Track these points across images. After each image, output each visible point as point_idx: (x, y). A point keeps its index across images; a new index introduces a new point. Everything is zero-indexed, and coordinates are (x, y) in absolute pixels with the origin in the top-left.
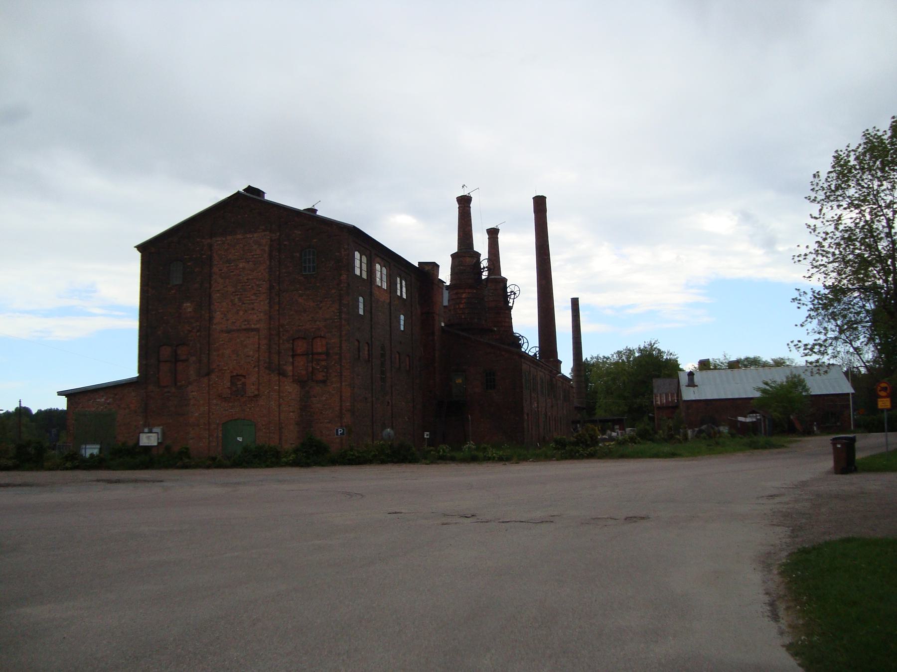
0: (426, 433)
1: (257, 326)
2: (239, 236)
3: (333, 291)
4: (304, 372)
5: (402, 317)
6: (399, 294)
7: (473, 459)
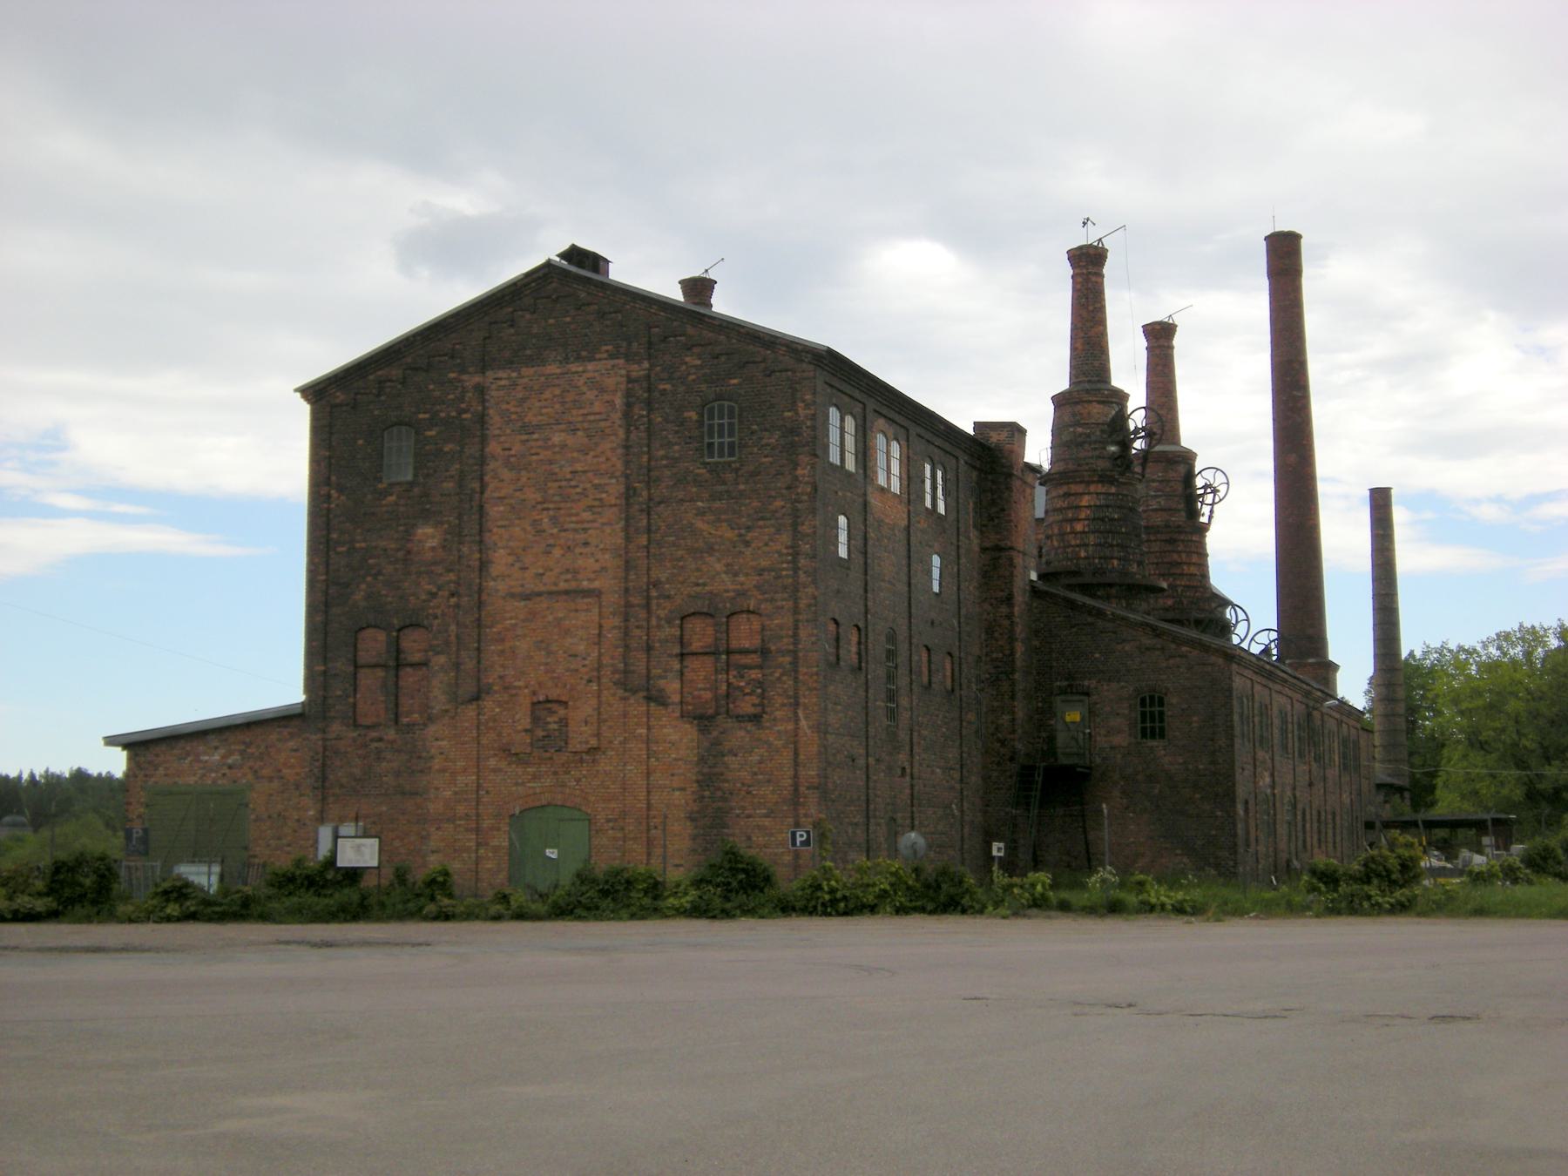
0: (995, 845)
1: (596, 584)
2: (553, 369)
3: (779, 503)
4: (708, 695)
5: (936, 560)
6: (928, 504)
7: (1114, 908)
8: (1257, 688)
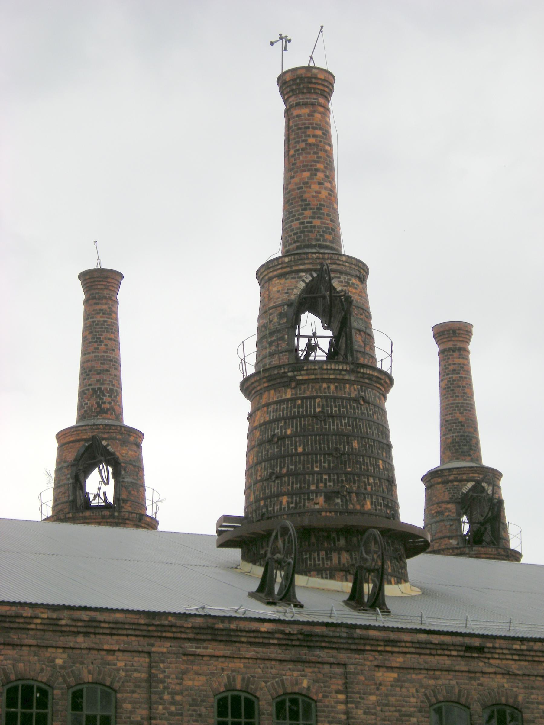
8: (169, 669)
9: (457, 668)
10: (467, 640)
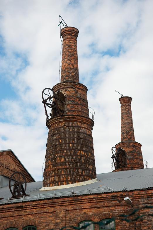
9: (14, 215)
10: (16, 205)
